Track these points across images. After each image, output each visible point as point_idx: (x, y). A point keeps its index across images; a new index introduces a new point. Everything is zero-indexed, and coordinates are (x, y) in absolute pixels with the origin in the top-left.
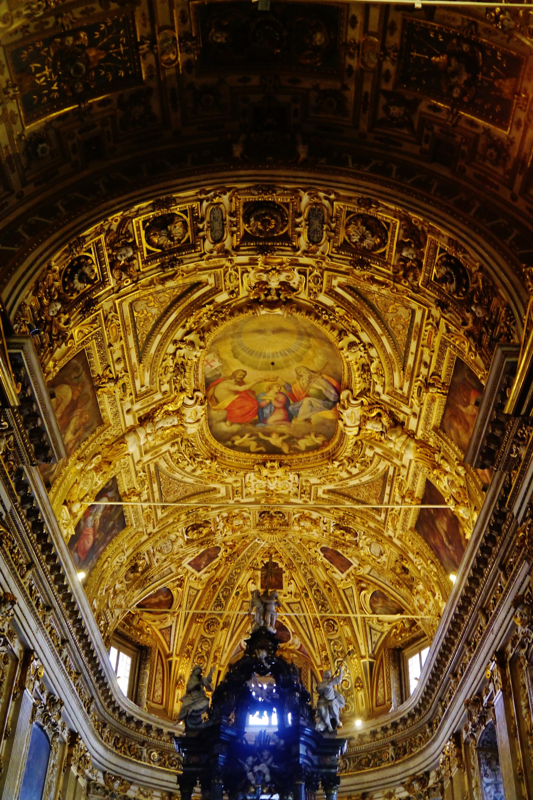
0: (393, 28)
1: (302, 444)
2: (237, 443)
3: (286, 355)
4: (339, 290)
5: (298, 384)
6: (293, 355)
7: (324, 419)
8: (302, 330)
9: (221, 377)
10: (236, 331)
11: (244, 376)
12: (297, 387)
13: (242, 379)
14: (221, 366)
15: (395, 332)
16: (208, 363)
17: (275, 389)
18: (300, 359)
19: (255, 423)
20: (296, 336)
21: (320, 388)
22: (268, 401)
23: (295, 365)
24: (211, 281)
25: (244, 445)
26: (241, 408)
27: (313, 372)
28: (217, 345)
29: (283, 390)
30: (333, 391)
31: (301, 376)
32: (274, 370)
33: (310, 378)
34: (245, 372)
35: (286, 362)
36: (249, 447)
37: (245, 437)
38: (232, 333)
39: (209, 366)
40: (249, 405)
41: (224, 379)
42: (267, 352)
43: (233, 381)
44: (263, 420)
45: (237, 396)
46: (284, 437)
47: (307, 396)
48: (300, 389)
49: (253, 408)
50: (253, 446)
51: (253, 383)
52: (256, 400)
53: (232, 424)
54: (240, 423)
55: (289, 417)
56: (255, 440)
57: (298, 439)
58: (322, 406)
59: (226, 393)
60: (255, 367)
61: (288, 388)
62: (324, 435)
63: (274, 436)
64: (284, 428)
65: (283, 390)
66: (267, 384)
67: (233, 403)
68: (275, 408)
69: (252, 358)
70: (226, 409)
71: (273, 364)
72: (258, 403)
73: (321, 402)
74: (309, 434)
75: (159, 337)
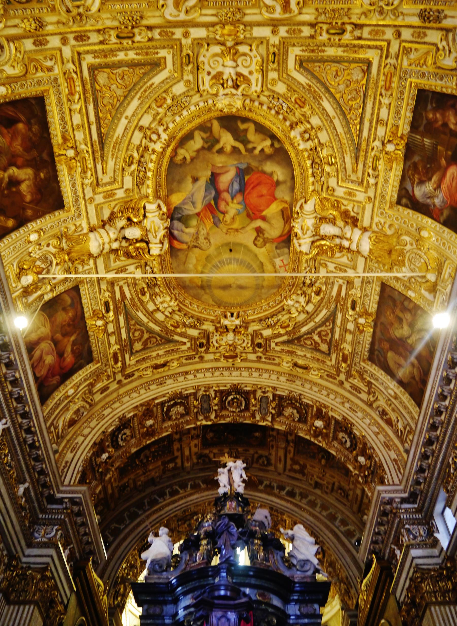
0: (178, 450)
1: (197, 143)
2: (268, 142)
3: (220, 262)
4: (185, 340)
5: (208, 228)
6: (214, 262)
7: (179, 191)
8: (208, 291)
9: (275, 244)
10: (259, 291)
11: (256, 239)
12: (209, 223)
13: (258, 236)
14: (275, 258)
15: (139, 327)
16: (285, 266)
17: (228, 217)
18: (208, 258)
19: (248, 170)
20: (213, 283)
21: (187, 230)
22: (235, 201)
23: (211, 251)
24: (273, 345)
25: (261, 136)
26: (262, 196)
27: (196, 247)
28: (276, 283)
29: (221, 216)
30: (176, 232)
31: (205, 239)
32: (229, 243)
33: (197, 238)
34: (255, 245)
35: (219, 254)
36: (256, 130)
37: (259, 148)
38: (263, 291)
39: (285, 262)
40: (253, 199)
41: (273, 240)
42: (235, 266)
43: (266, 235)
44: (241, 173)
45: (264, 213)
46: (217, 147)
47: (198, 214)
48: (206, 221)
49: (249, 193)
50: (252, 136)
51: (248, 229)
52: (246, 204)
53: (271, 174)
54: (264, 172)
55: (214, 179)
56: (249, 142)
57: (203, 148)
58: (183, 206)
59: (273, 222)
60: (246, 247)
61: (216, 220)
62: (177, 164)
63: (228, 149)
64: (219, 160)
65: (221, 216)
66: (235, 226)
67: (268, 206)
68: (228, 191)
69: (248, 259)
70: (275, 199)
71: (231, 250)
72: (244, 199)
73: (186, 213)
74: (192, 159)
75: (317, 319)
